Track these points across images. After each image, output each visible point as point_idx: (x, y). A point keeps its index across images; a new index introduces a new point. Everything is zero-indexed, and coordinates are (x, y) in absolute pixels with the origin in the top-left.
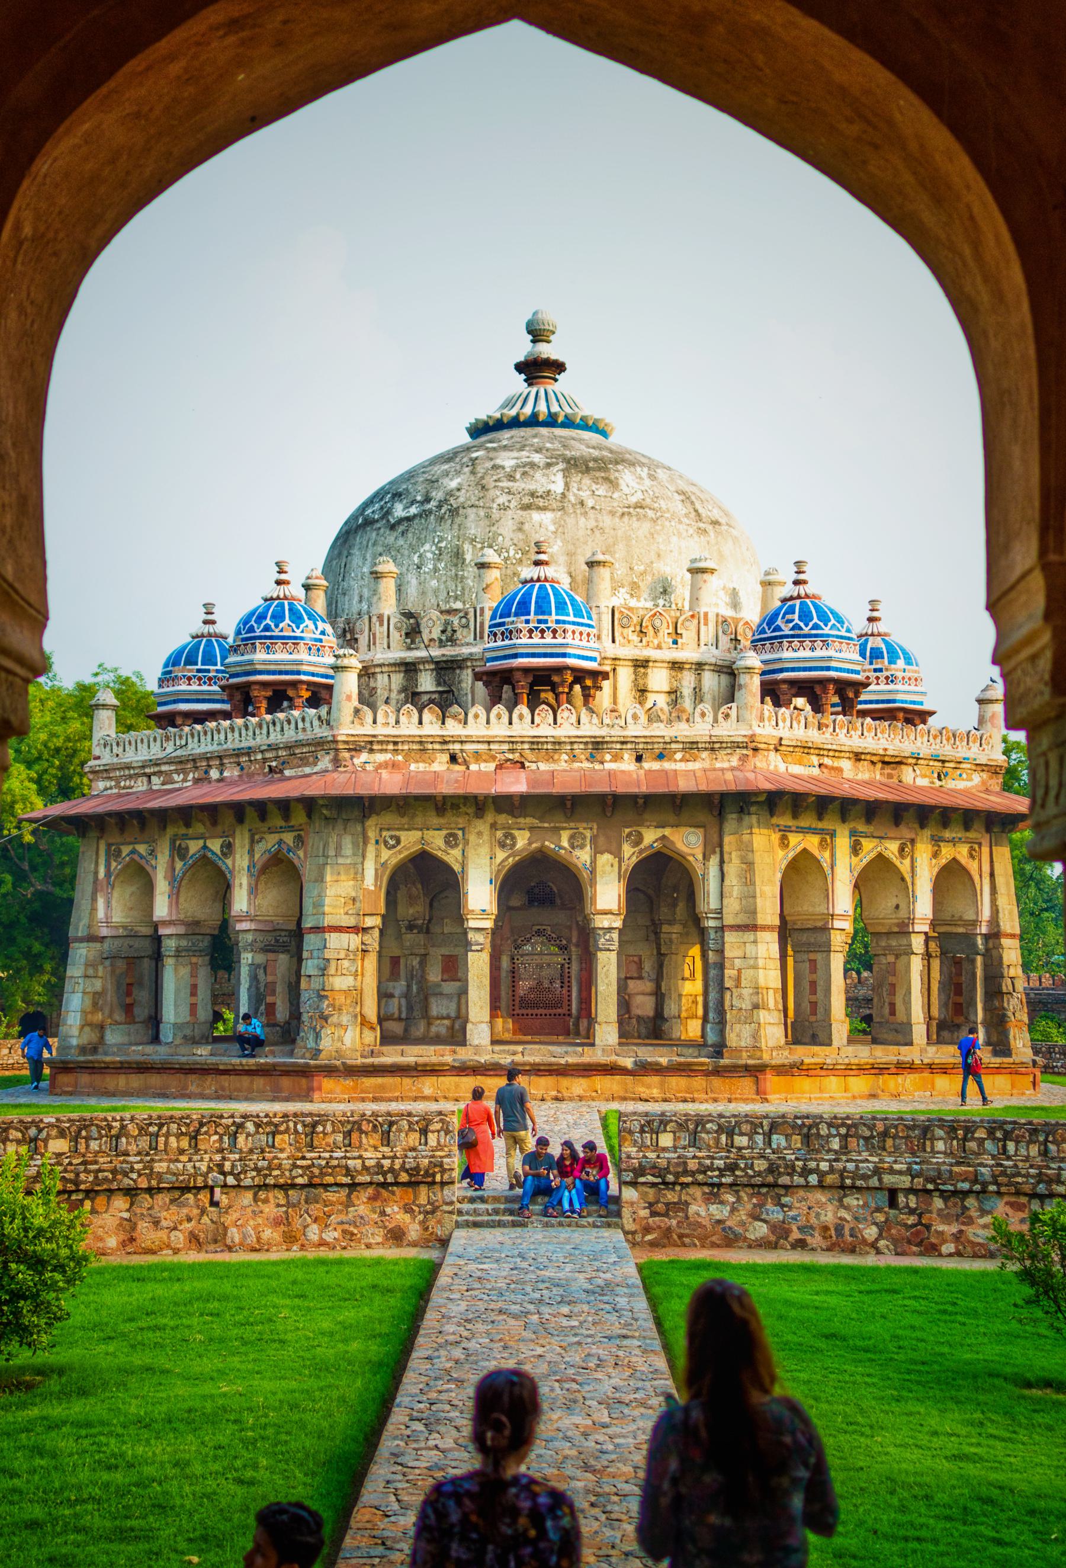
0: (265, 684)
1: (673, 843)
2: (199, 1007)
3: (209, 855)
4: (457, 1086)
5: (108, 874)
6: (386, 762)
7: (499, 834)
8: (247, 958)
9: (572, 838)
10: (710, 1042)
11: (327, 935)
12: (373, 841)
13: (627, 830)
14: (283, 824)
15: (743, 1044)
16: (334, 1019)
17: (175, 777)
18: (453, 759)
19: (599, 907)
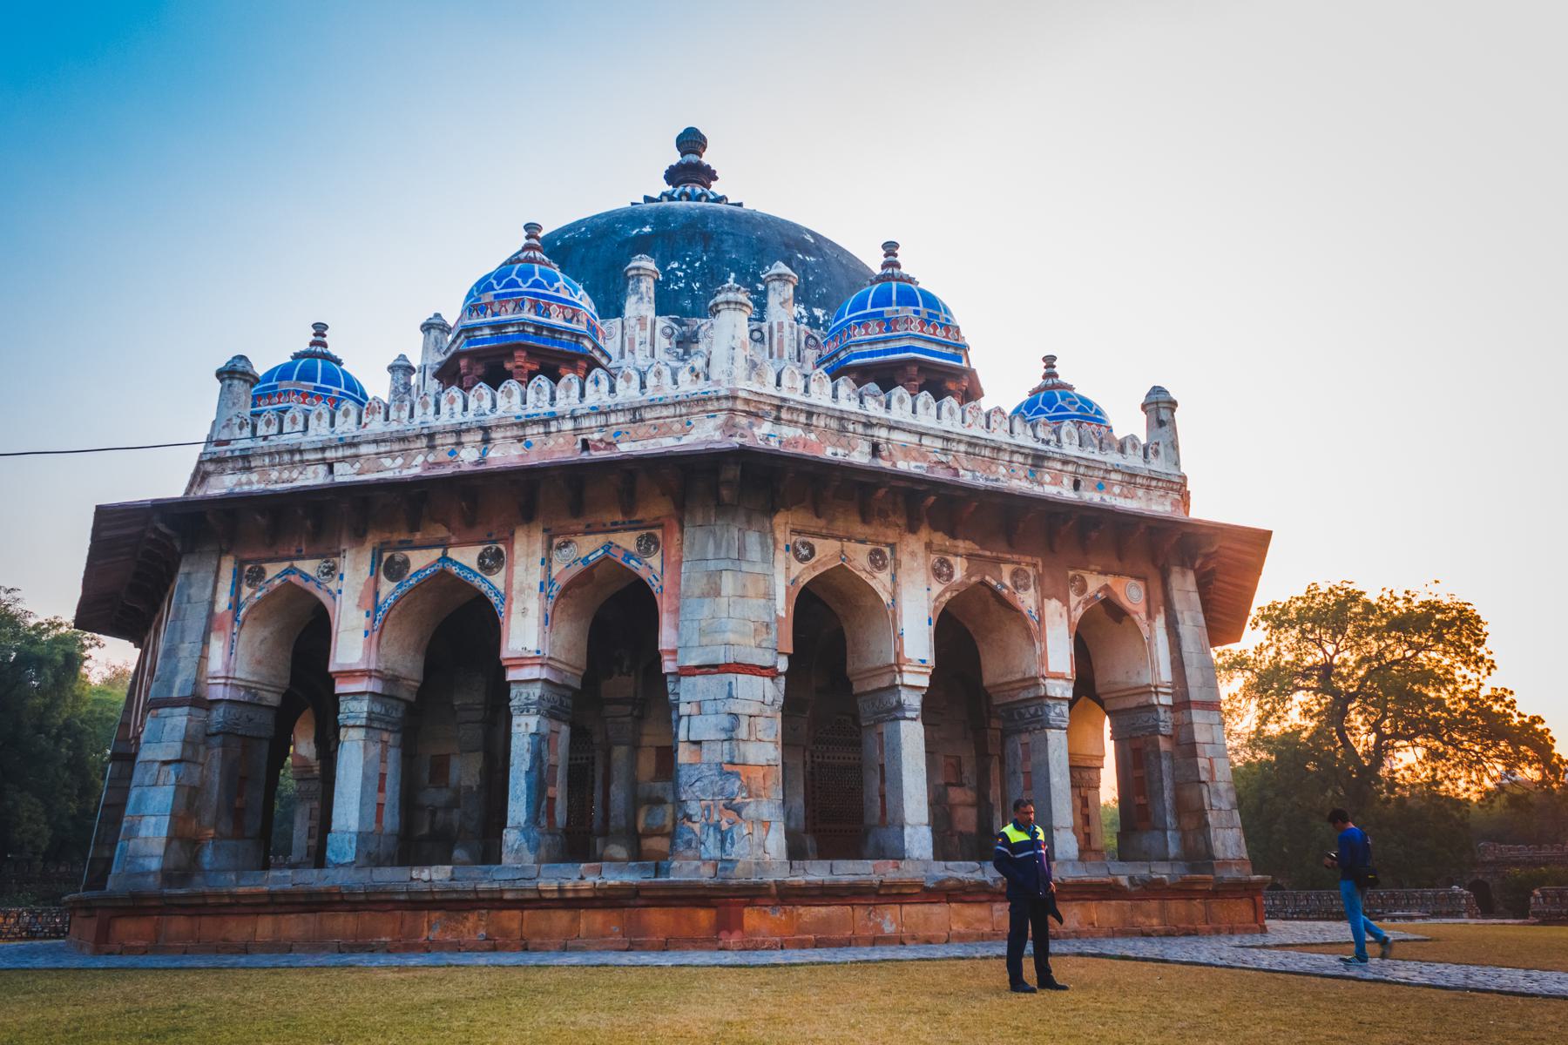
0: (532, 352)
1: (1115, 594)
2: (386, 809)
3: (455, 570)
4: (927, 919)
5: (235, 605)
6: (794, 438)
7: (934, 558)
8: (525, 726)
9: (1014, 574)
10: (1171, 855)
11: (731, 677)
12: (782, 546)
13: (1071, 573)
14: (619, 517)
15: (1230, 856)
16: (749, 811)
17: (387, 462)
18: (875, 450)
19: (1051, 669)
